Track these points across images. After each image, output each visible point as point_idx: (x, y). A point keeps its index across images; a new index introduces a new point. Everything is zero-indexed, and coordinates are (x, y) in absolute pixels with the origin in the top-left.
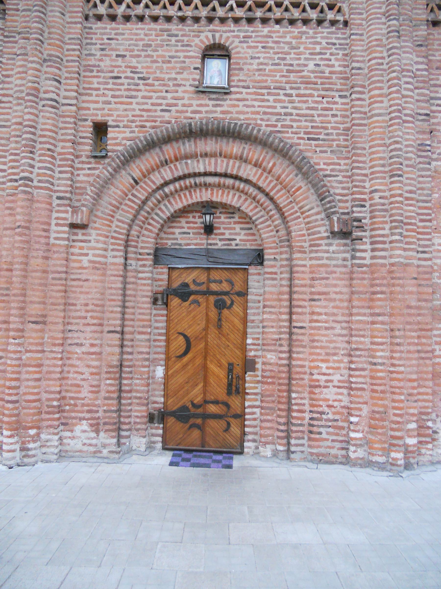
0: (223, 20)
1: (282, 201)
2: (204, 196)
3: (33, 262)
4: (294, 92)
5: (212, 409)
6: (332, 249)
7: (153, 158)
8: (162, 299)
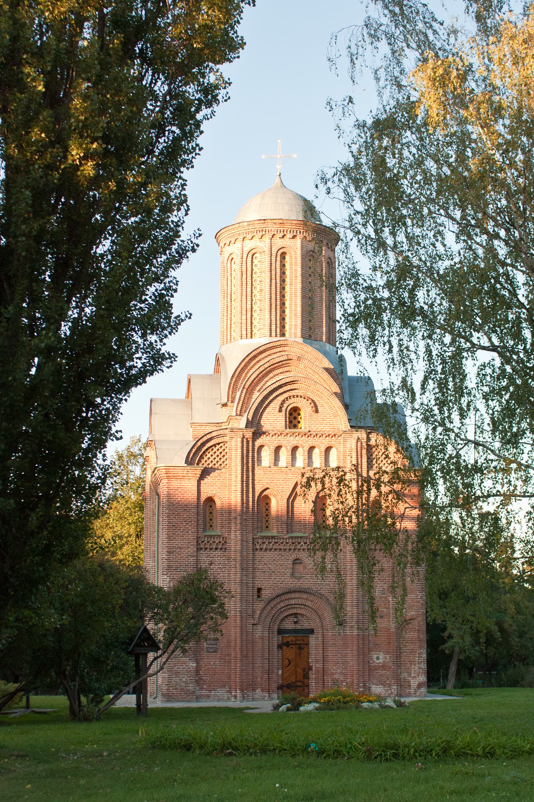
0: (299, 550)
1: (320, 613)
2: (294, 611)
5: (298, 684)
7: (278, 600)
8: (280, 647)
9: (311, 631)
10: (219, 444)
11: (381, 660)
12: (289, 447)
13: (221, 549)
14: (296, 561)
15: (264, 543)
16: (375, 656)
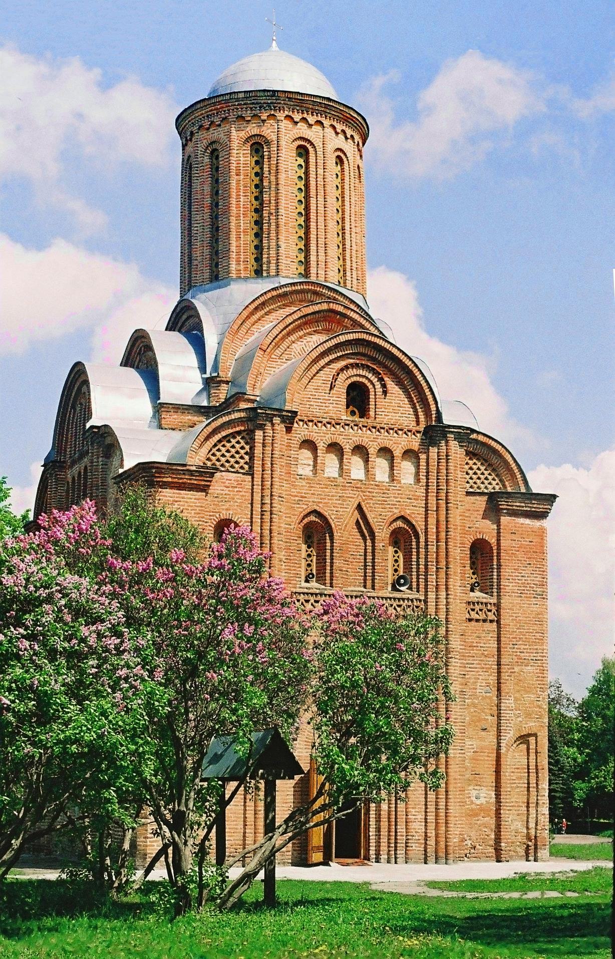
11: (482, 800)
12: (348, 447)
15: (307, 601)
16: (474, 793)
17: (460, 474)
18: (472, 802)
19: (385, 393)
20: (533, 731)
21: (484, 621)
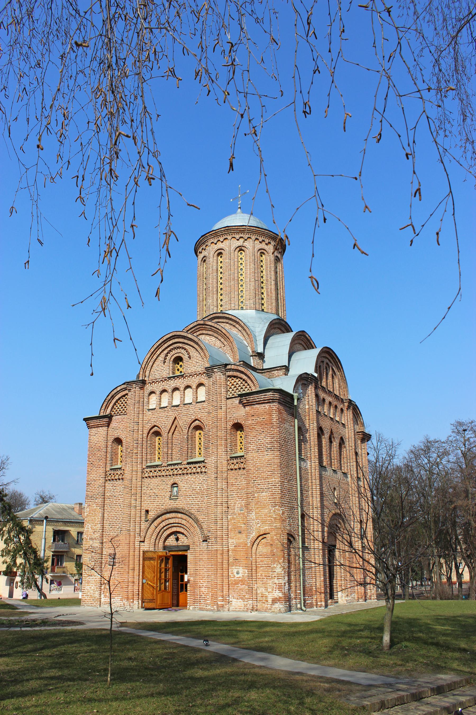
0: (177, 475)
2: (174, 529)
3: (131, 553)
4: (194, 497)
6: (204, 545)
7: (159, 520)
9: (187, 548)
10: (124, 396)
11: (240, 575)
13: (122, 479)
14: (174, 485)
15: (151, 472)
16: (235, 571)
17: (223, 390)
18: (234, 575)
19: (190, 357)
20: (268, 531)
21: (240, 469)
